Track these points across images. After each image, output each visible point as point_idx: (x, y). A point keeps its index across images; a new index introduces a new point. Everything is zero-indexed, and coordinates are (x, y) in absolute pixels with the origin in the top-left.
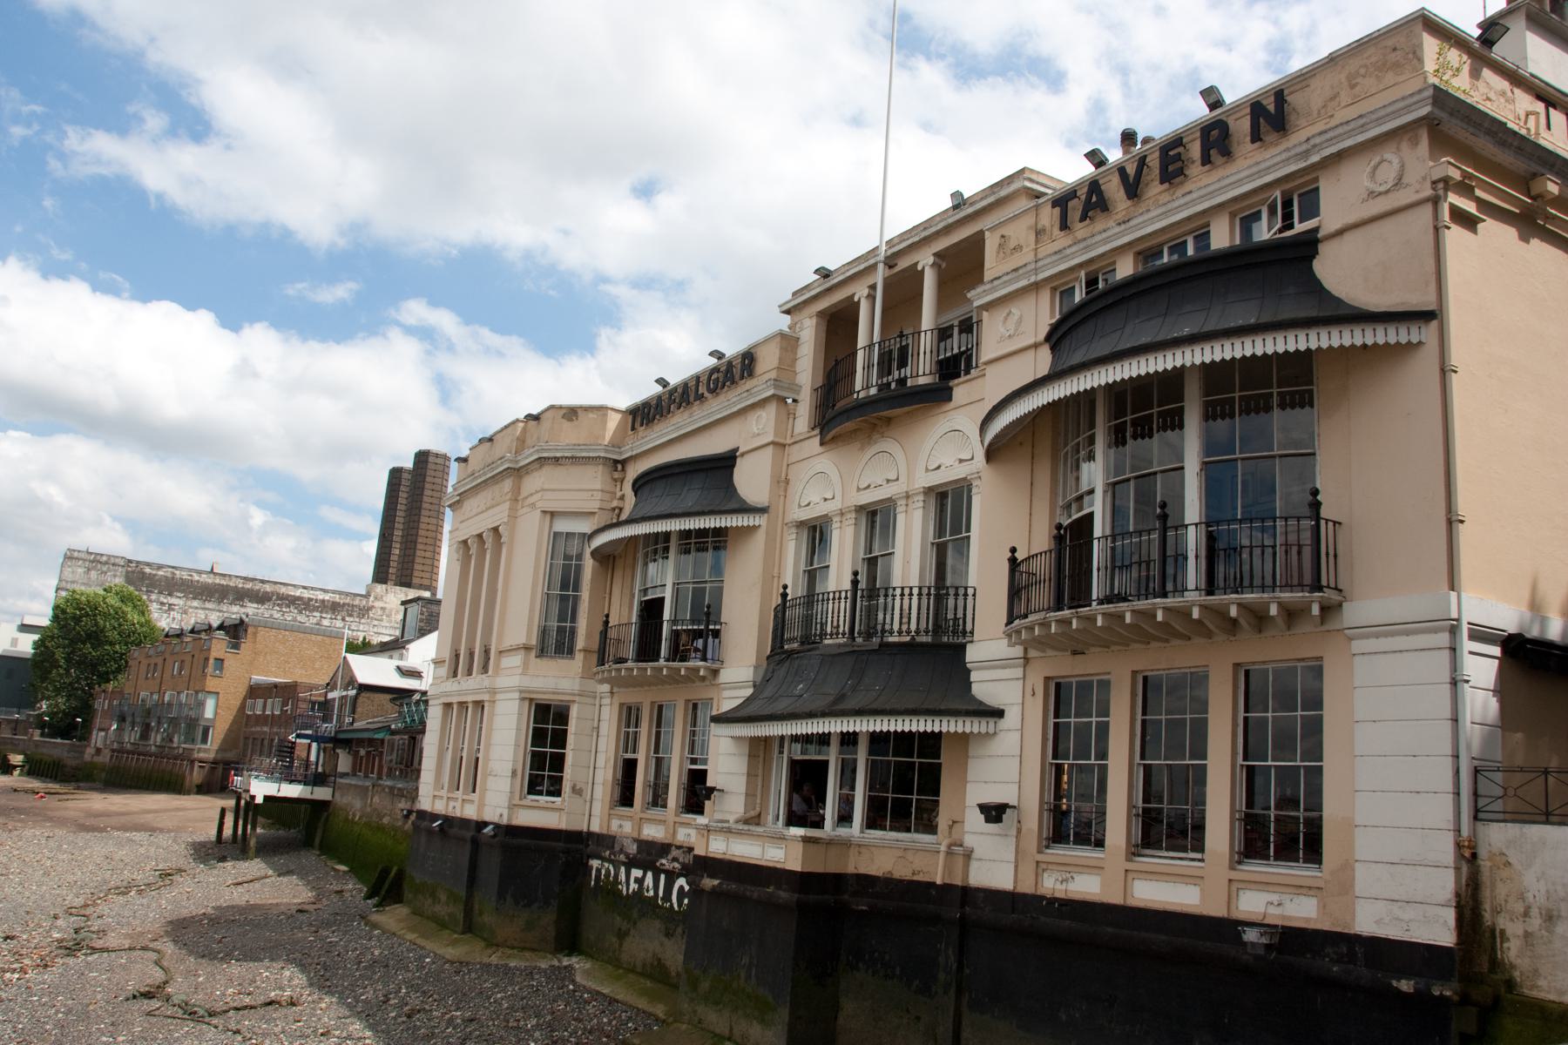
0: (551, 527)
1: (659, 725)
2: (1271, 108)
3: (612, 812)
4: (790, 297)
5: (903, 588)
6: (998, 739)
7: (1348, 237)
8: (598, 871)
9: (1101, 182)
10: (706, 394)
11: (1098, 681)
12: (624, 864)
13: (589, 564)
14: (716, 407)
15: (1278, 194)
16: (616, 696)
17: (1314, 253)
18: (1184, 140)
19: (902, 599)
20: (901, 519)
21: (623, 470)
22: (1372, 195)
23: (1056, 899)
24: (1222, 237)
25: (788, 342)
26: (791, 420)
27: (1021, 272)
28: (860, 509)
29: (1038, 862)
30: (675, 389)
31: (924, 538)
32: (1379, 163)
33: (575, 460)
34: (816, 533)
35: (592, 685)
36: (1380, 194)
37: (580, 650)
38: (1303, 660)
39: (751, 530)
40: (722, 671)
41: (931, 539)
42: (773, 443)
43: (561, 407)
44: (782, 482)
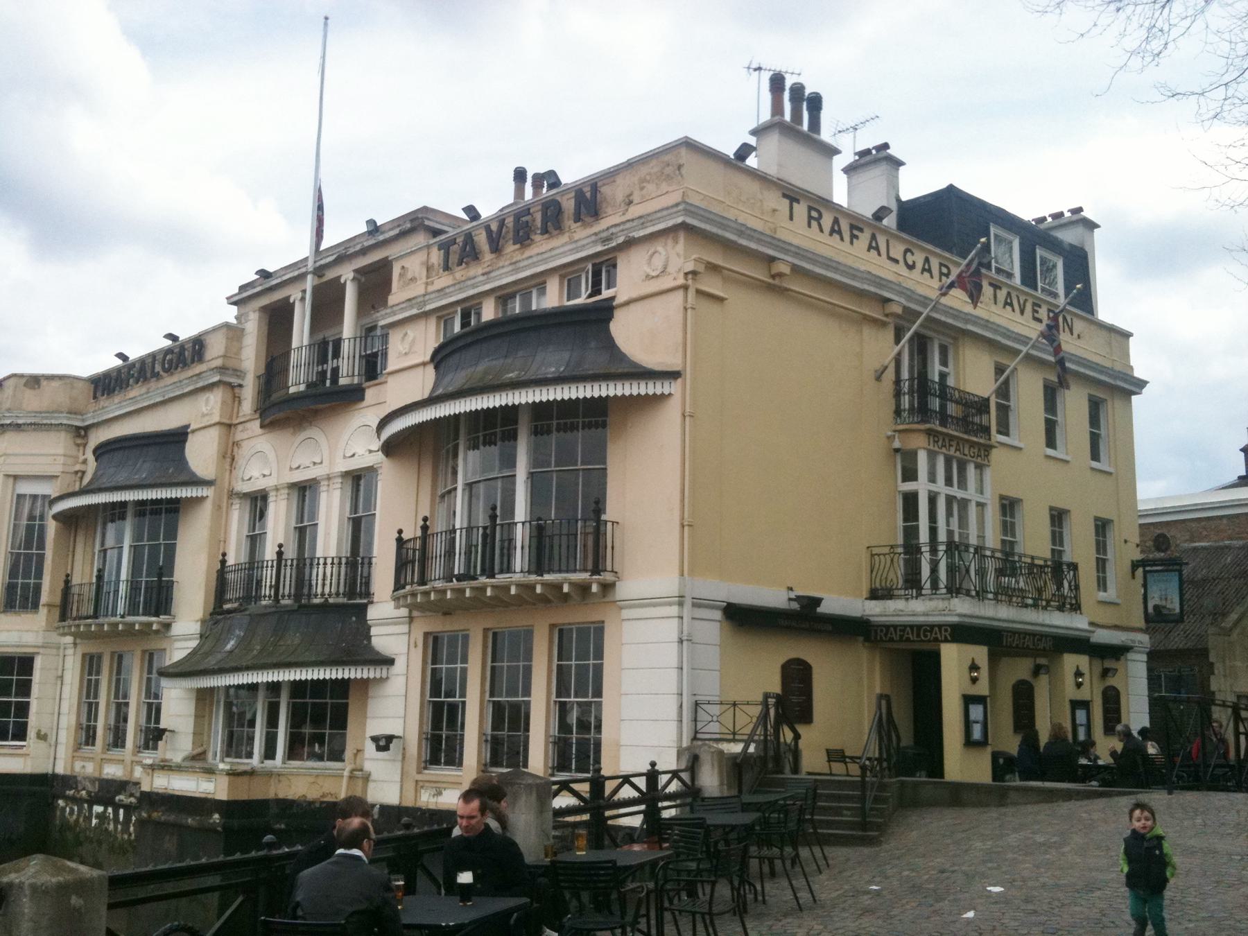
0: (14, 489)
1: (119, 672)
2: (588, 195)
3: (75, 754)
4: (237, 291)
5: (325, 559)
6: (389, 681)
7: (632, 307)
8: (63, 809)
9: (473, 234)
10: (162, 373)
11: (463, 635)
12: (87, 801)
13: (52, 527)
14: (169, 384)
15: (590, 267)
16: (79, 647)
18: (531, 211)
19: (325, 568)
20: (323, 497)
21: (86, 436)
22: (649, 277)
23: (429, 810)
24: (552, 298)
25: (233, 332)
26: (237, 402)
27: (414, 302)
28: (292, 486)
29: (417, 781)
30: (133, 365)
31: (341, 515)
32: (654, 253)
33: (37, 427)
34: (258, 502)
35: (54, 638)
36: (653, 277)
37: (44, 605)
38: (594, 623)
39: (199, 500)
40: (173, 625)
41: (347, 514)
42: (219, 423)
43: (22, 376)
44: (229, 455)
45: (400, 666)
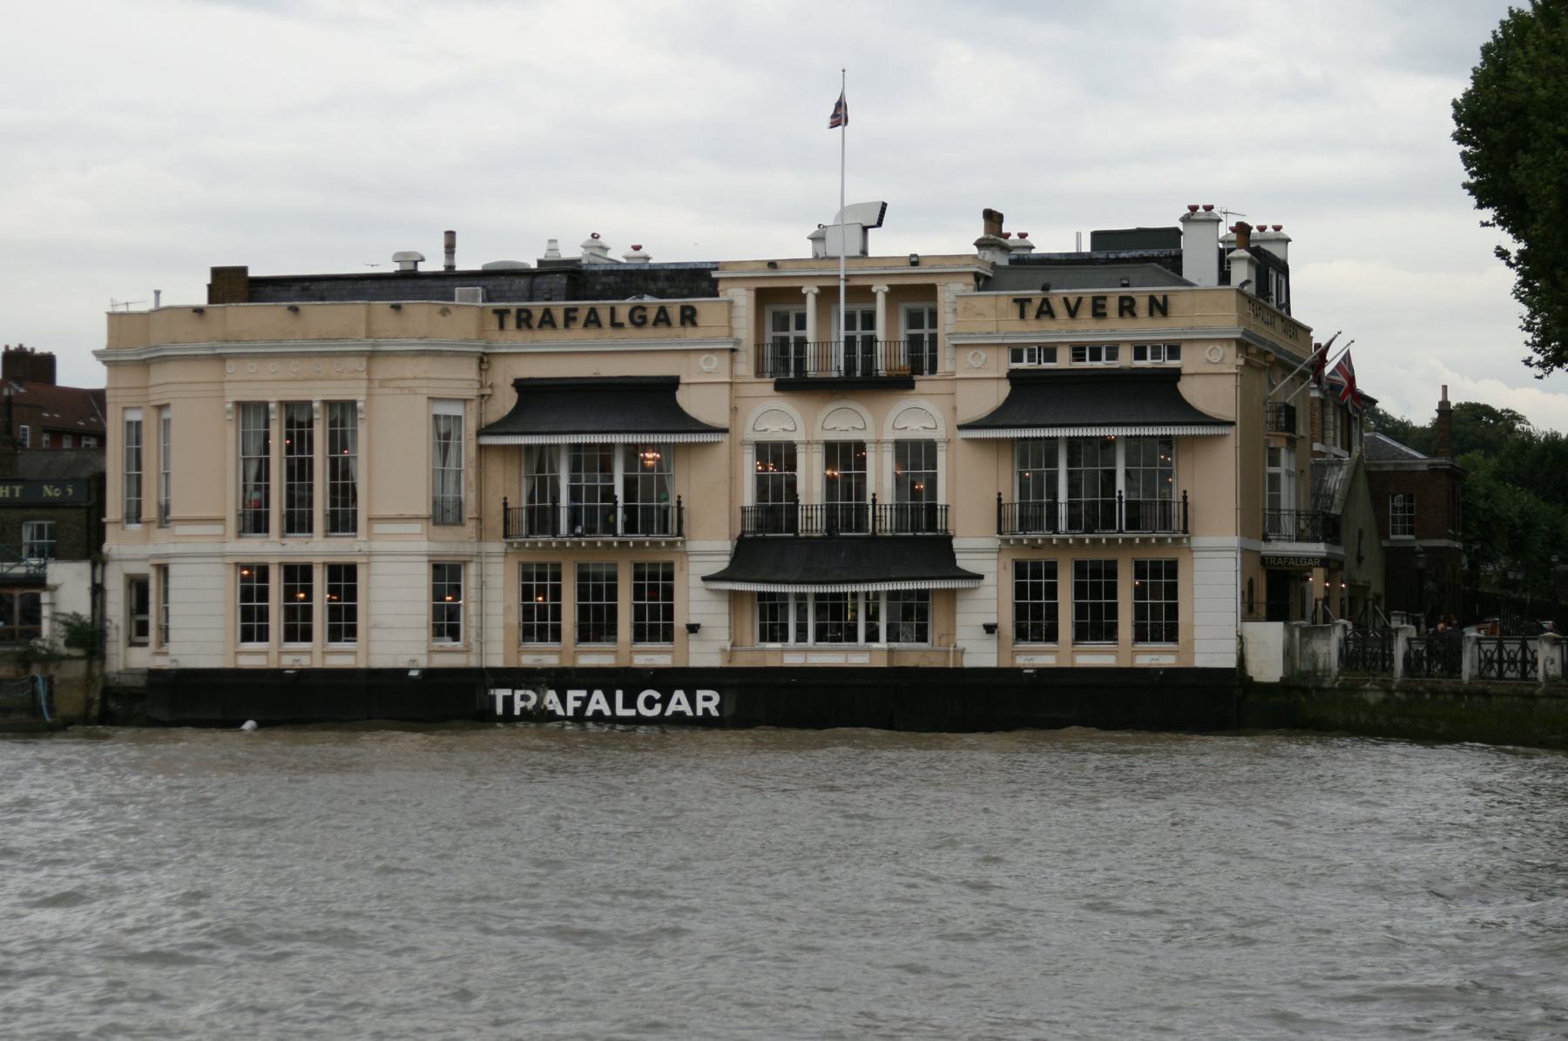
17: (1179, 380)
22: (1209, 362)
45: (990, 579)
